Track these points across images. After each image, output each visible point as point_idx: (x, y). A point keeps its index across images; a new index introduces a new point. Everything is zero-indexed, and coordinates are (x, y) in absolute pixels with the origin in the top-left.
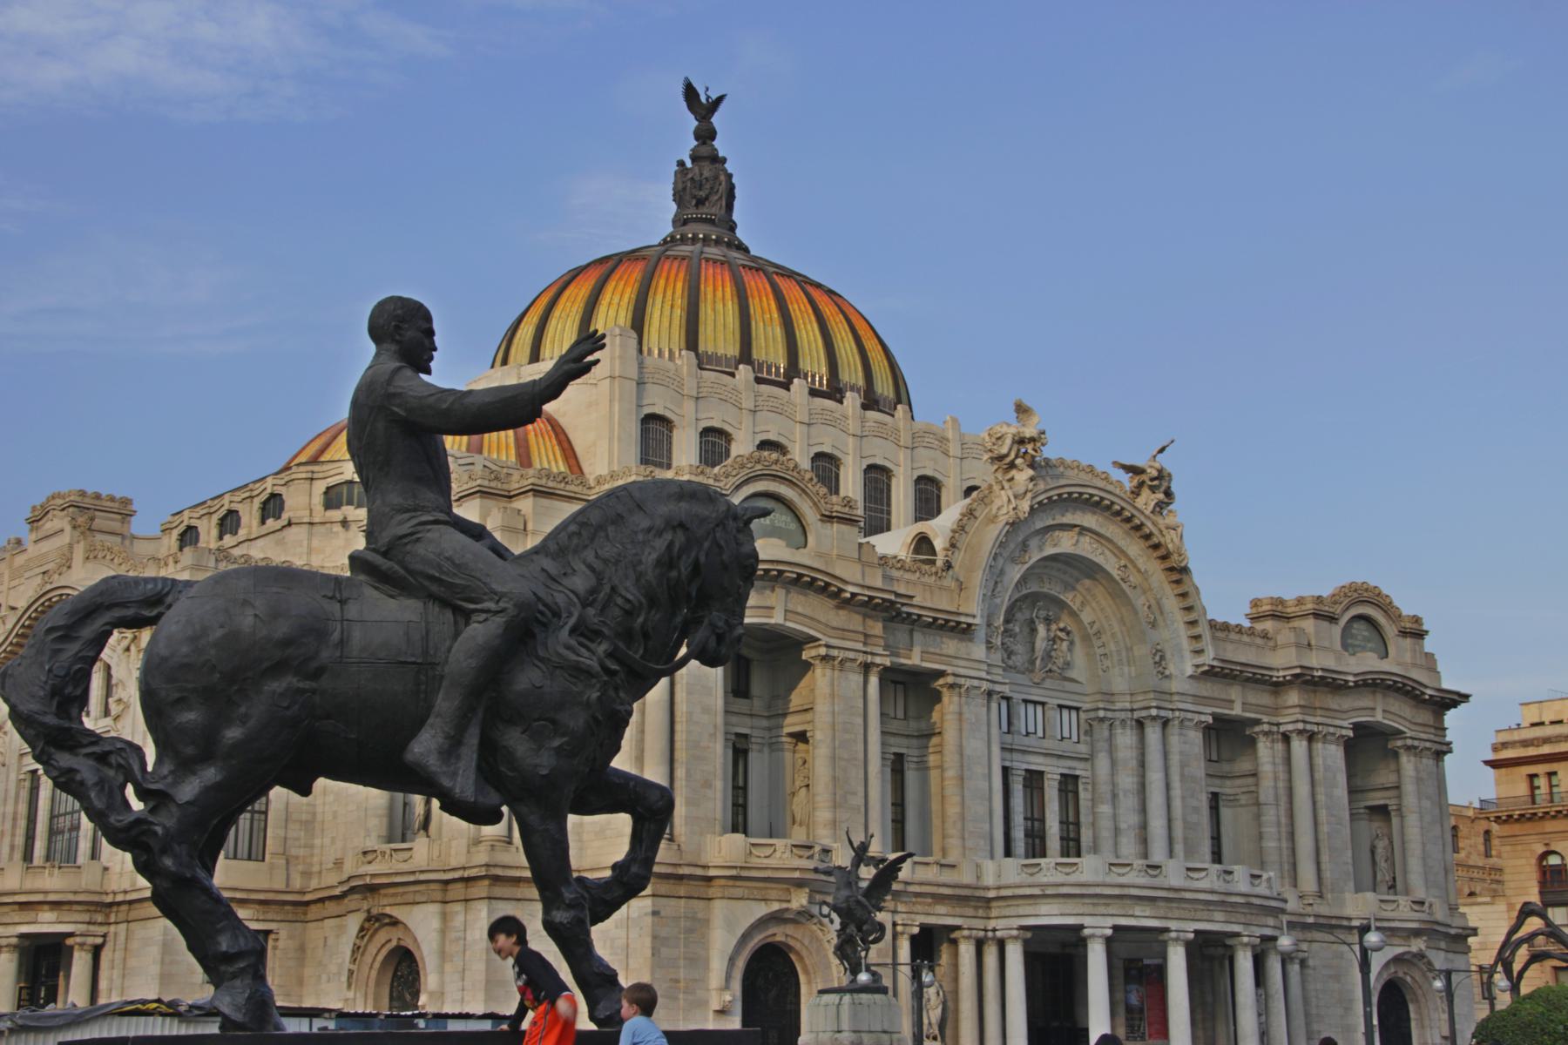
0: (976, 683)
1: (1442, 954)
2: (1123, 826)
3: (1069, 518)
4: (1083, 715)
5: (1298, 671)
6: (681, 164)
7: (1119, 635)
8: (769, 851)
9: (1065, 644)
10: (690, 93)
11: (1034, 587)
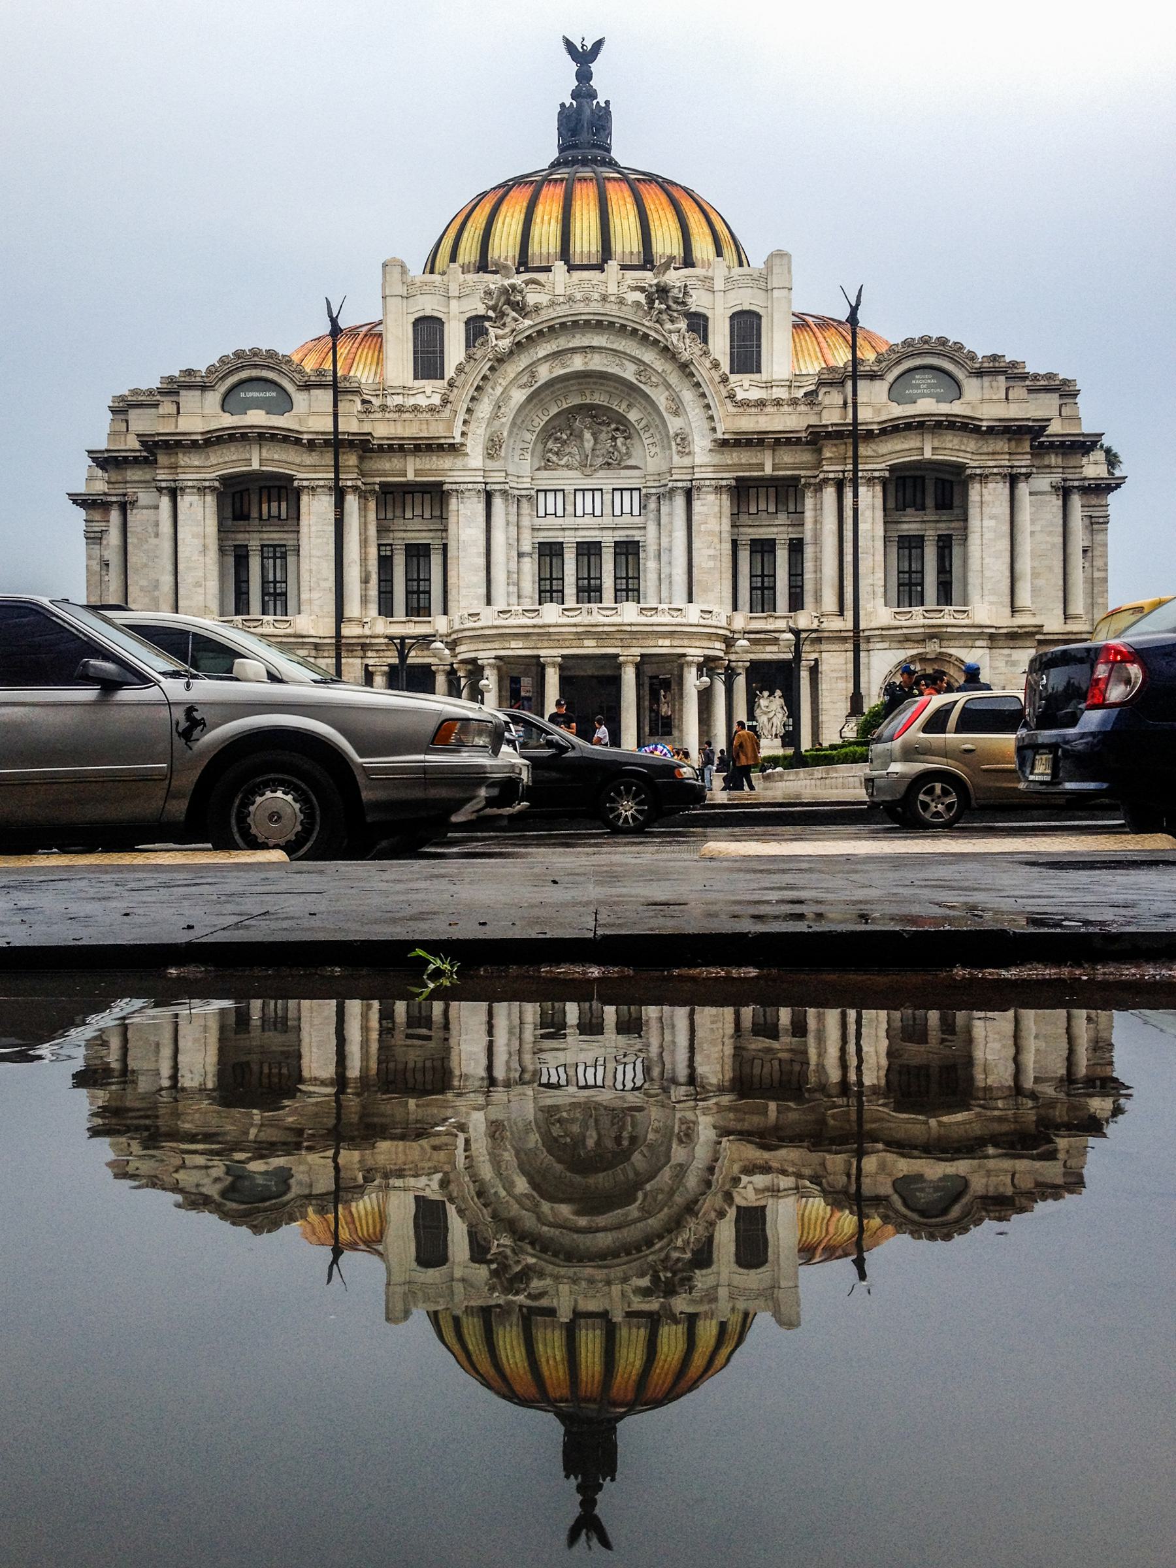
0: (470, 486)
2: (663, 576)
5: (811, 430)
6: (562, 105)
7: (661, 427)
9: (619, 441)
10: (569, 46)
11: (576, 400)
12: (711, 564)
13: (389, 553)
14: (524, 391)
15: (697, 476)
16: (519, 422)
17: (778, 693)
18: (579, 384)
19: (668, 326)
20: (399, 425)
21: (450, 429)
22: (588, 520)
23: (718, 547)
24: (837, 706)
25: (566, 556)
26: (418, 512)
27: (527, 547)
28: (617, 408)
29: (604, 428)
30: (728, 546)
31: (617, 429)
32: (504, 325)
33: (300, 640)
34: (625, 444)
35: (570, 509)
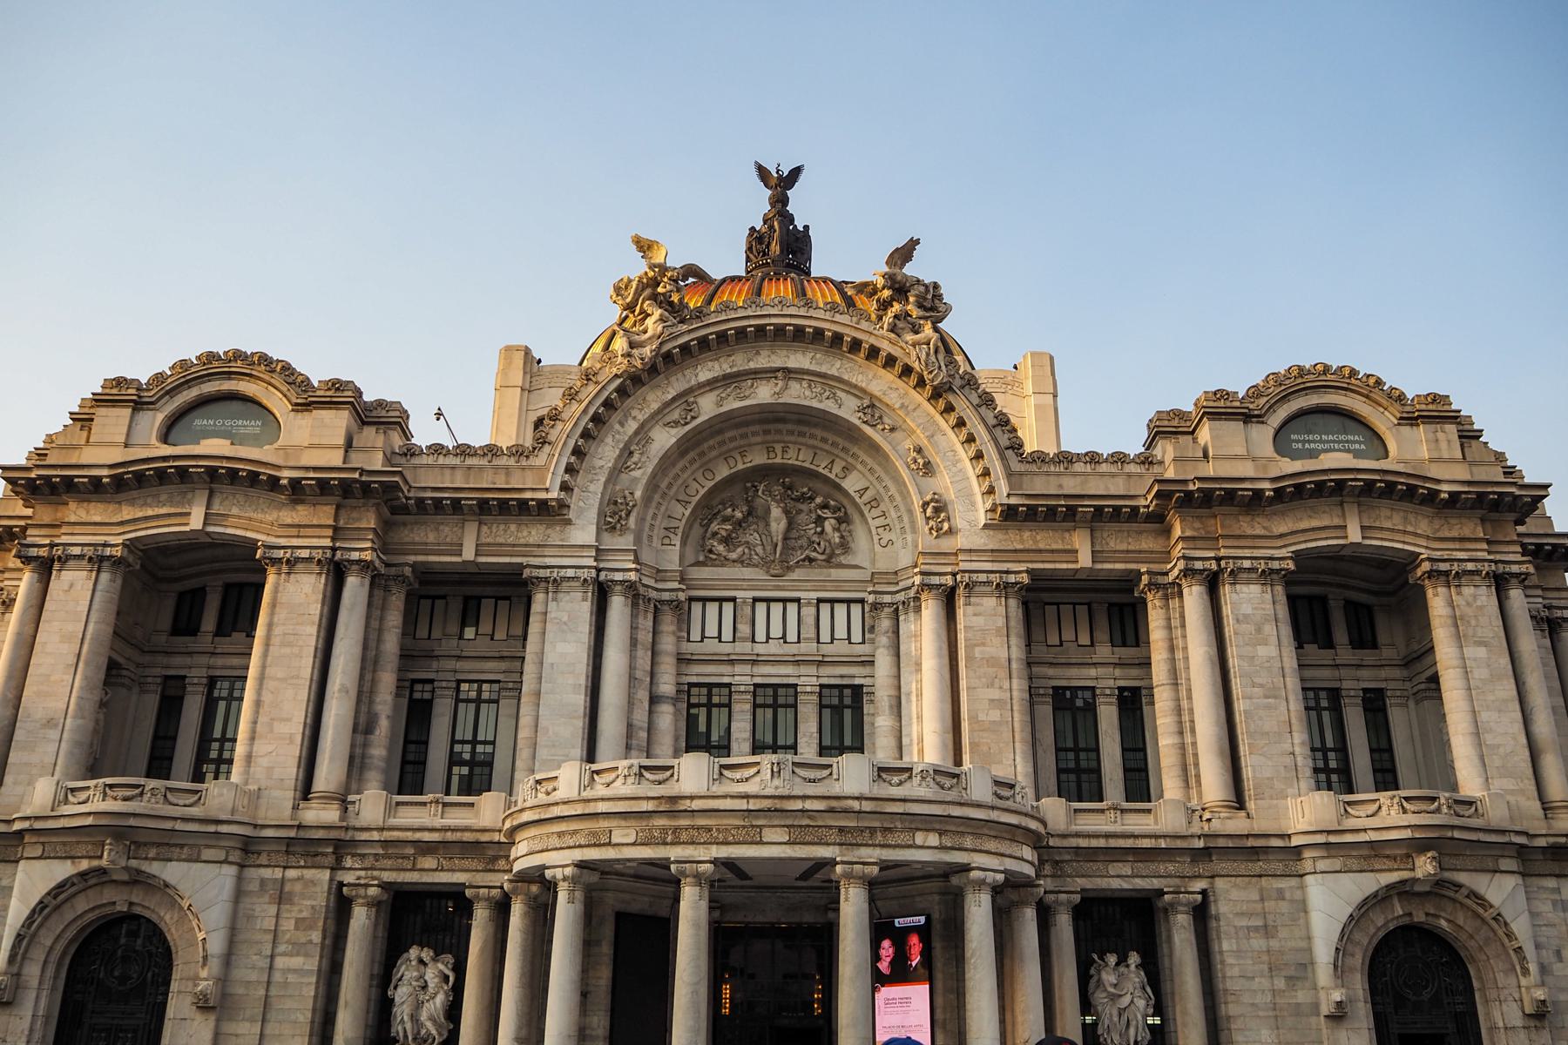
1: (1510, 882)
3: (764, 360)
4: (867, 608)
6: (753, 229)
7: (898, 498)
8: (83, 796)
9: (828, 526)
10: (763, 172)
11: (758, 458)
12: (995, 715)
13: (427, 696)
14: (673, 431)
15: (963, 566)
16: (663, 485)
17: (1134, 959)
18: (767, 432)
19: (910, 337)
20: (459, 474)
21: (543, 480)
22: (774, 648)
23: (1006, 685)
24: (1255, 985)
25: (736, 707)
26: (486, 627)
27: (667, 686)
28: (825, 472)
29: (804, 507)
30: (1019, 686)
31: (825, 506)
32: (645, 332)
33: (212, 828)
34: (838, 530)
35: (744, 629)
